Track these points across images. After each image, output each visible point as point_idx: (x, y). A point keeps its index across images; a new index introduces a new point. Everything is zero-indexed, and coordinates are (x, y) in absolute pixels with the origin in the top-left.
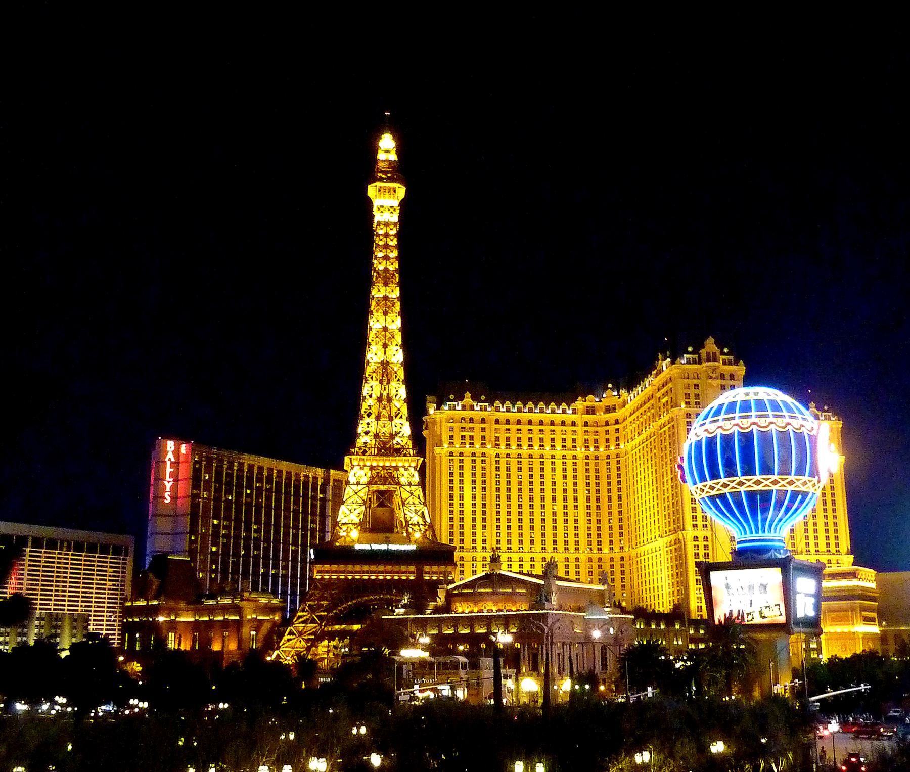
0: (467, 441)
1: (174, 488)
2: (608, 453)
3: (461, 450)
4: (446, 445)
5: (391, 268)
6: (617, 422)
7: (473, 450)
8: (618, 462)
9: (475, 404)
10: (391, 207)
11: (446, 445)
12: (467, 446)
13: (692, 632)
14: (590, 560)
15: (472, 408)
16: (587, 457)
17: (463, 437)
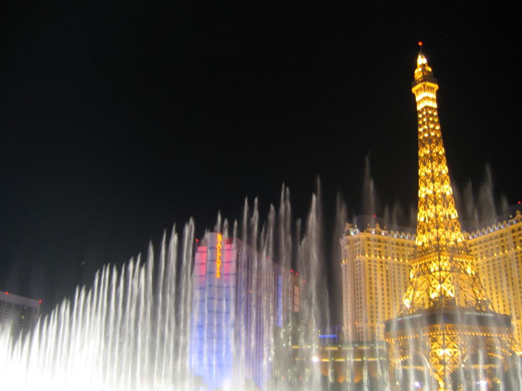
0: (378, 253)
1: (221, 267)
3: (375, 259)
4: (367, 256)
5: (438, 135)
9: (382, 231)
10: (433, 99)
11: (367, 256)
12: (378, 257)
15: (380, 233)
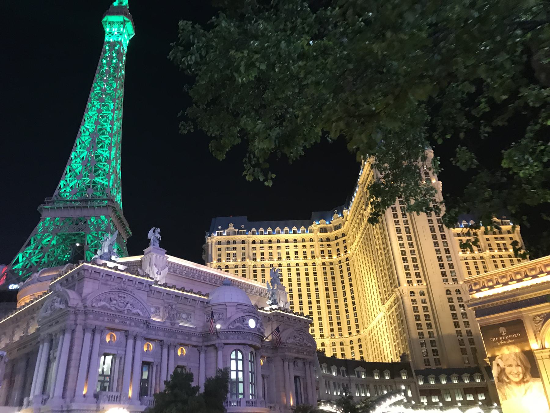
2: (339, 259)
3: (227, 264)
6: (343, 235)
7: (236, 263)
8: (348, 264)
13: (421, 383)
14: (334, 344)
16: (324, 264)
17: (228, 255)
